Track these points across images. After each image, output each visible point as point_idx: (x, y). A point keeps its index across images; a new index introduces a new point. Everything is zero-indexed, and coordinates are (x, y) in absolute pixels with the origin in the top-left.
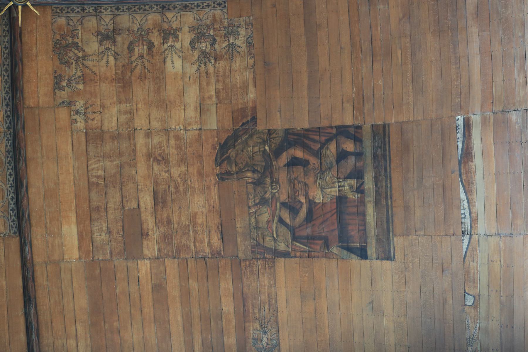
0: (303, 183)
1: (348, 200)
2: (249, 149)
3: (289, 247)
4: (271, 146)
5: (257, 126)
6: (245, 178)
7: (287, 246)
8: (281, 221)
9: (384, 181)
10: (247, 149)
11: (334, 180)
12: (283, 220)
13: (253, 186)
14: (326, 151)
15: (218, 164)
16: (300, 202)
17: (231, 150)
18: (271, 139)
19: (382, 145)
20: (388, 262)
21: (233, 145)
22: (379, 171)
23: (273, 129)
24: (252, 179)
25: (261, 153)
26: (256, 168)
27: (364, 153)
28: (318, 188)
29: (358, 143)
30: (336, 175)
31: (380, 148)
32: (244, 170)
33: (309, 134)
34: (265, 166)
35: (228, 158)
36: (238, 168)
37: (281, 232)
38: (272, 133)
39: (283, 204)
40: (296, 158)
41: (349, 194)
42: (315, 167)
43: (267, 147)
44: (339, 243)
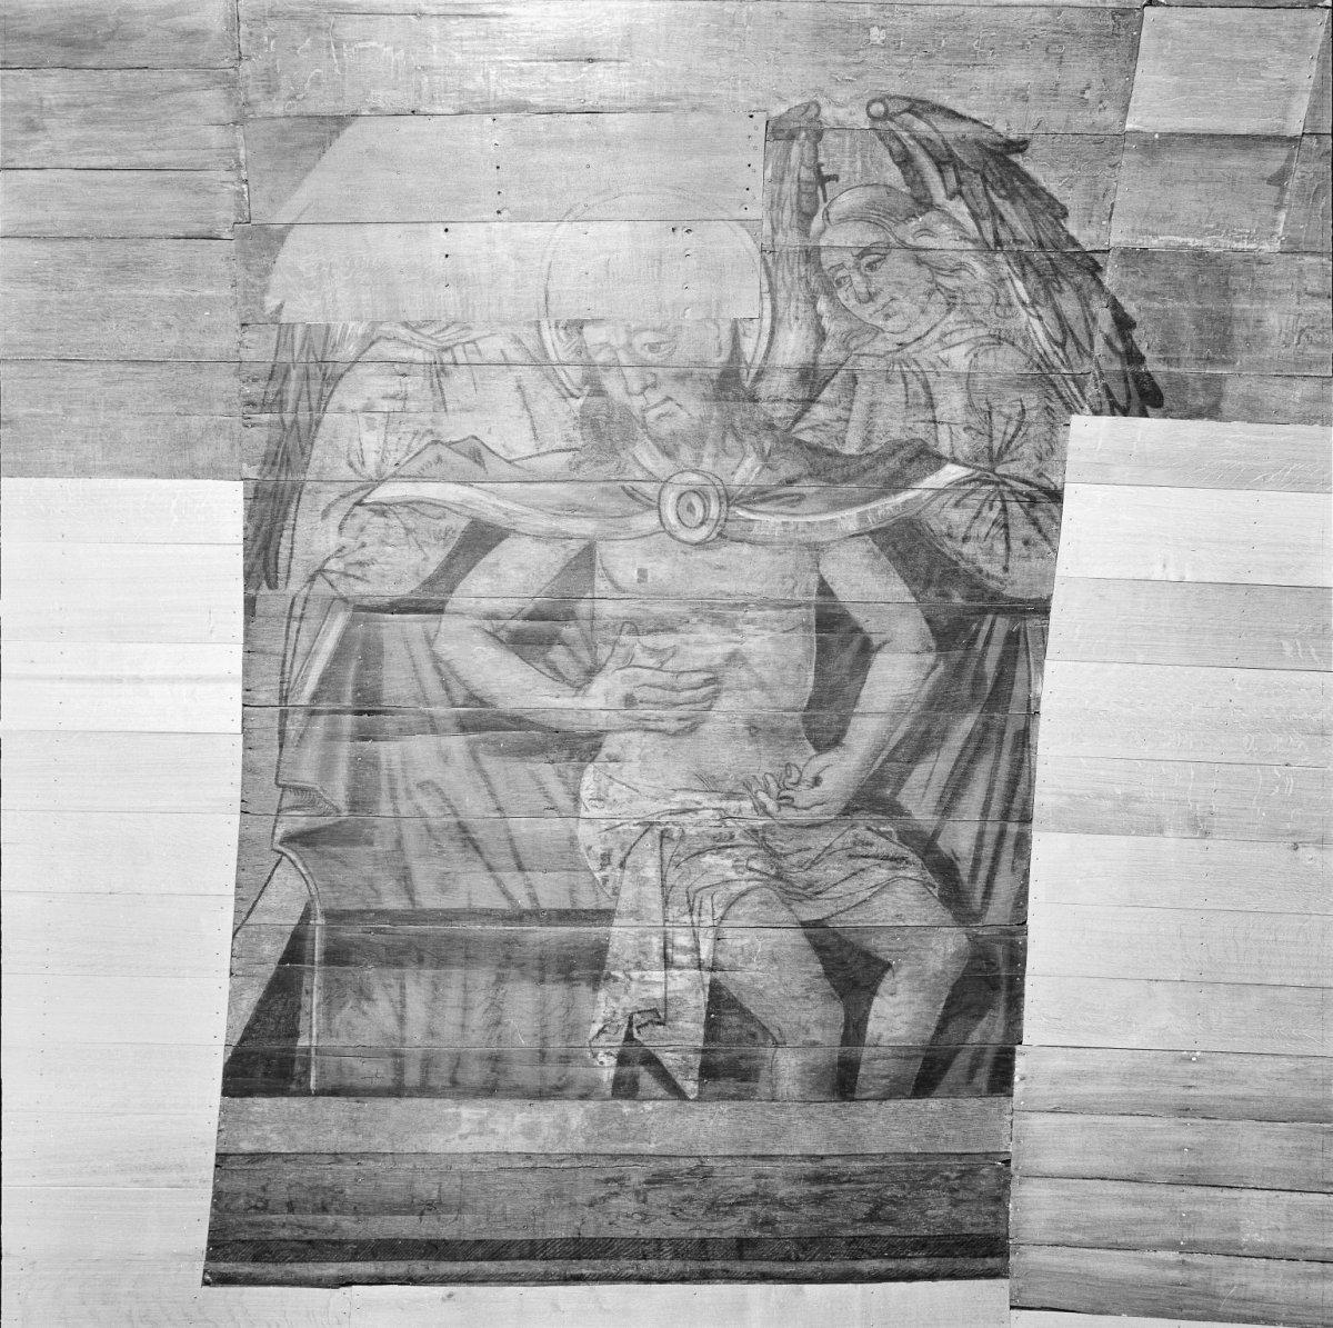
0: (705, 698)
1: (584, 990)
2: (959, 358)
3: (312, 579)
4: (956, 505)
5: (1096, 413)
6: (774, 309)
7: (321, 571)
8: (480, 539)
9: (678, 1229)
10: (956, 338)
11: (707, 903)
12: (489, 548)
13: (719, 360)
14: (886, 858)
15: (887, 116)
16: (591, 673)
17: (970, 224)
18: (998, 504)
19: (887, 1230)
20: (201, 1240)
21: (998, 242)
22: (739, 1204)
23: (1059, 524)
24: (758, 361)
25: (921, 432)
26: (826, 394)
27: (853, 1106)
28: (666, 797)
29: (915, 1067)
30: (737, 917)
31: (872, 1217)
32: (822, 306)
33: (998, 755)
34: (834, 454)
35: (924, 203)
36: (842, 266)
37: (408, 531)
38: (1039, 514)
39: (586, 560)
40: (867, 650)
41: (617, 999)
42: (797, 784)
43: (952, 473)
44: (327, 914)
